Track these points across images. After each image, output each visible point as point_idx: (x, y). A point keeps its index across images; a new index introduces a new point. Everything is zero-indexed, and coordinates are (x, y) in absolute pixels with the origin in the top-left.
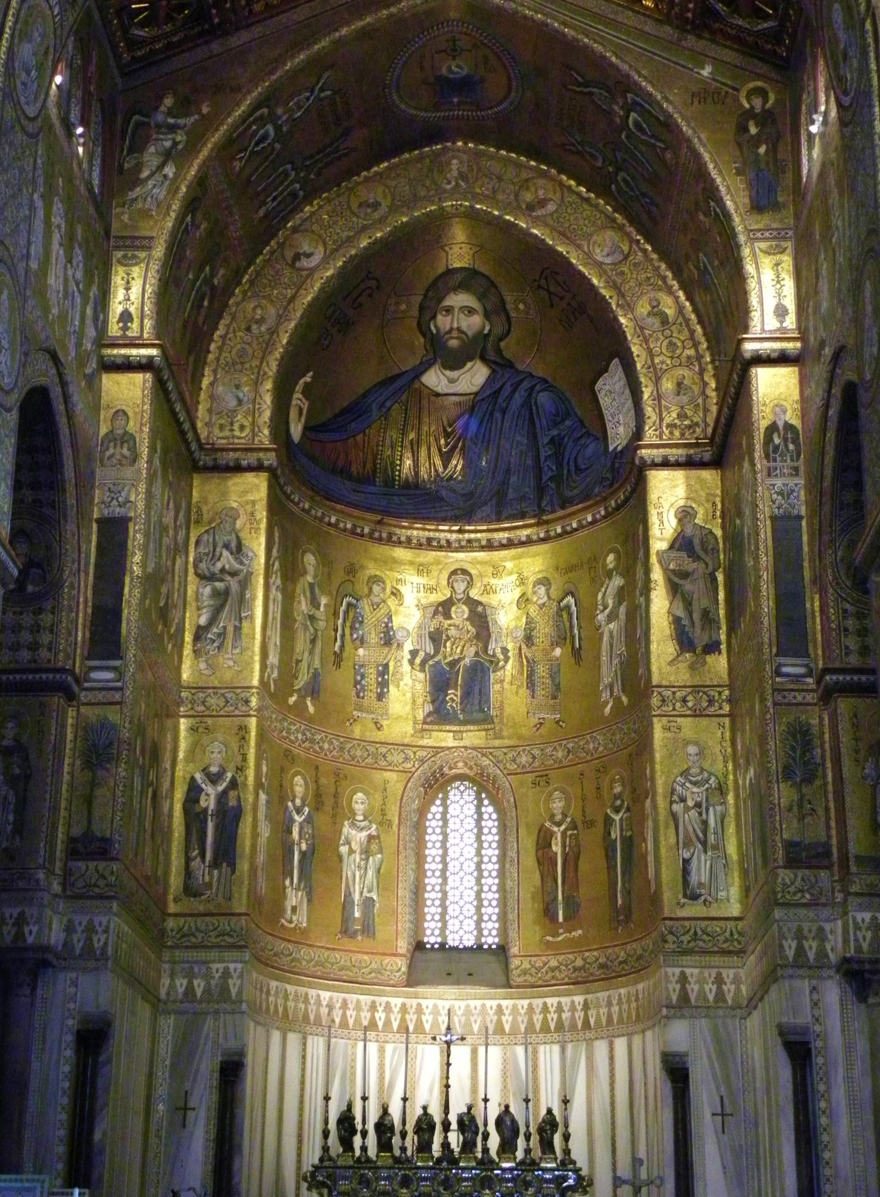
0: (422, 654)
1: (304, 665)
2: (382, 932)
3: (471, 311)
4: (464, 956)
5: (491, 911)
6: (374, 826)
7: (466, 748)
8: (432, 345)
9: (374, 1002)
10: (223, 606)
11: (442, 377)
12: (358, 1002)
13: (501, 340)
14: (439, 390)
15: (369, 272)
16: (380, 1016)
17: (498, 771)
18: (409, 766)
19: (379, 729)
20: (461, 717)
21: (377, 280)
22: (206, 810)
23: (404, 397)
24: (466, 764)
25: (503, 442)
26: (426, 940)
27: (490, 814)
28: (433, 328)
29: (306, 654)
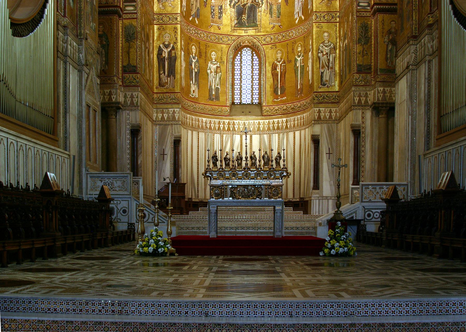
0: (233, 2)
2: (222, 99)
4: (249, 106)
5: (256, 91)
6: (219, 63)
7: (248, 36)
9: (219, 121)
12: (215, 121)
16: (222, 126)
17: (259, 44)
18: (230, 42)
19: (219, 29)
20: (247, 24)
24: (248, 42)
26: (235, 101)
27: (256, 59)
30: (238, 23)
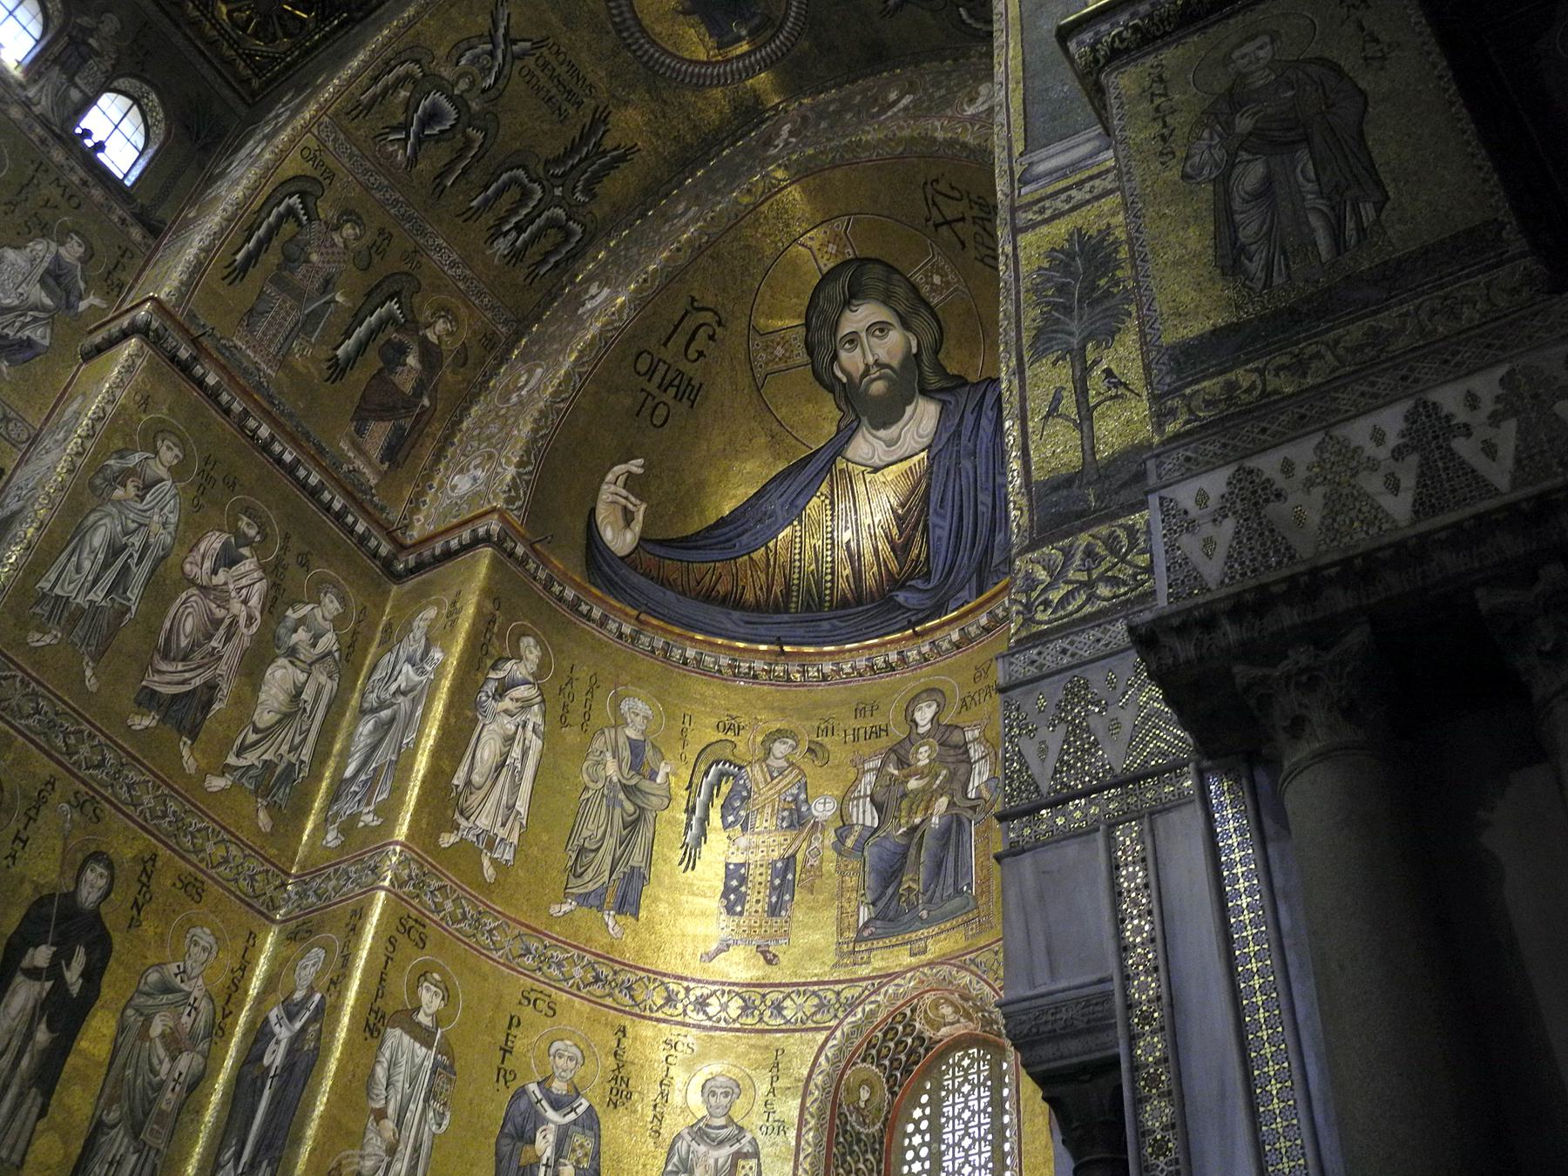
1: (605, 858)
3: (882, 328)
7: (931, 964)
8: (848, 401)
10: (381, 740)
11: (875, 442)
13: (937, 352)
14: (879, 463)
15: (693, 299)
17: (987, 989)
19: (769, 962)
20: (924, 914)
21: (716, 313)
22: (269, 1068)
23: (824, 488)
25: (981, 497)
28: (839, 374)
29: (610, 843)
30: (876, 918)
